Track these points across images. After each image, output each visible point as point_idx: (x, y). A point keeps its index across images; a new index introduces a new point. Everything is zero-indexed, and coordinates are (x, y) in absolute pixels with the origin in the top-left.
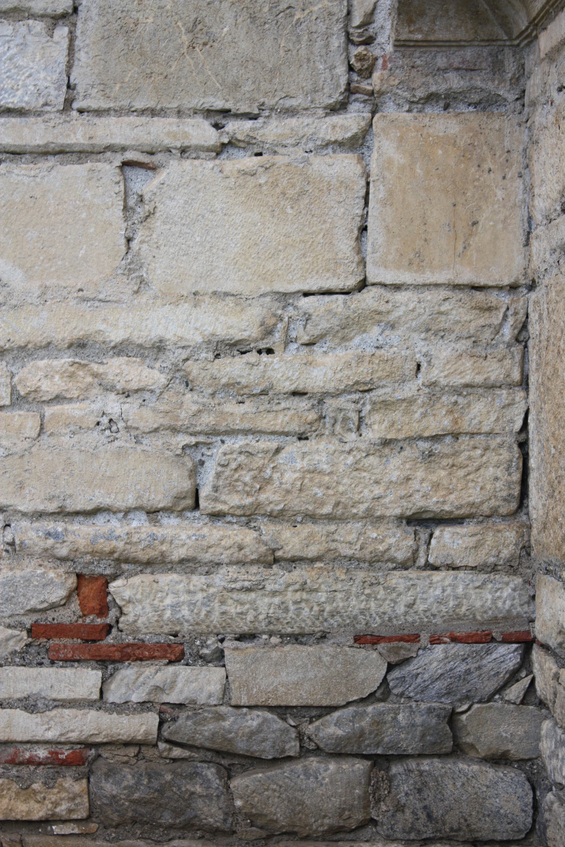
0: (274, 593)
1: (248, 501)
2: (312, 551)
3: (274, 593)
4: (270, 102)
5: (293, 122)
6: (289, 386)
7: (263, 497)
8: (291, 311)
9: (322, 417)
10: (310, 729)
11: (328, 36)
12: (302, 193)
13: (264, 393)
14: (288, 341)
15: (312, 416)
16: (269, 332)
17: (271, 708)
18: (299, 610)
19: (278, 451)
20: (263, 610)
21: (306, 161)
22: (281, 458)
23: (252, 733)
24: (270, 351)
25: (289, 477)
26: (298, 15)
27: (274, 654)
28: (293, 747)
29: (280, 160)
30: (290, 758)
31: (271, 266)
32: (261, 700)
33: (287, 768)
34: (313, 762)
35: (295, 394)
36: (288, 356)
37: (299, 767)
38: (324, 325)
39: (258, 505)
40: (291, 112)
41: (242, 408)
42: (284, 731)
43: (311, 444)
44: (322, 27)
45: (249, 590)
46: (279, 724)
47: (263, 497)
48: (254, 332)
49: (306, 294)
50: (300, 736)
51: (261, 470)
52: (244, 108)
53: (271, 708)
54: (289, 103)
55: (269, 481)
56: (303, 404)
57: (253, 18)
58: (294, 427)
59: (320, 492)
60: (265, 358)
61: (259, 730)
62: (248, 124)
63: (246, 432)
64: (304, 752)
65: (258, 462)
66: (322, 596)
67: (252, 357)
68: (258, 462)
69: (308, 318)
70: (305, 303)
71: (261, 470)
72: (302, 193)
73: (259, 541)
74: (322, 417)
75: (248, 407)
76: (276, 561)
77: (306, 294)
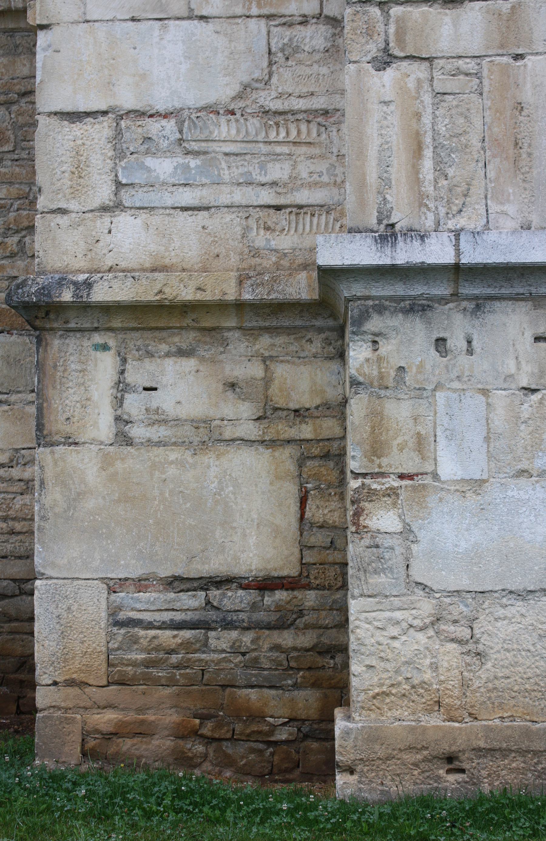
0: (12, 543)
1: (5, 514)
2: (24, 530)
3: (12, 543)
4: (13, 389)
5: (20, 395)
6: (17, 478)
7: (9, 513)
8: (19, 454)
9: (28, 488)
10: (23, 586)
11: (31, 369)
12: (22, 417)
13: (10, 480)
14: (17, 464)
15: (25, 487)
16: (12, 461)
17: (11, 580)
18: (20, 549)
19: (14, 498)
20: (9, 548)
21: (24, 407)
22: (15, 501)
23: (4, 588)
24: (12, 467)
25: (17, 506)
26: (22, 362)
27: (12, 562)
28: (17, 592)
29: (16, 407)
30: (16, 596)
31: (12, 440)
32: (8, 577)
33: (15, 598)
34: (24, 597)
35: (20, 480)
36: (17, 469)
37: (19, 598)
38: (29, 459)
39: (8, 515)
40: (19, 392)
41: (3, 485)
42: (15, 587)
43: (25, 496)
44: (29, 366)
45: (4, 542)
46: (13, 584)
47: (9, 513)
48: (7, 461)
49: (24, 449)
50: (20, 589)
51: (9, 504)
52: (5, 391)
53: (11, 580)
54: (18, 389)
55: (11, 508)
56: (22, 484)
57: (8, 363)
58: (19, 491)
59: (27, 511)
60: (10, 469)
61: (7, 586)
62: (6, 396)
63: (4, 492)
64: (21, 594)
65: (8, 502)
66: (27, 544)
67: (6, 469)
68: (8, 502)
69: (23, 456)
70: (23, 452)
71: (9, 504)
72: (22, 417)
73: (8, 527)
74: (28, 488)
75: (5, 485)
76: (13, 533)
77: (24, 449)
